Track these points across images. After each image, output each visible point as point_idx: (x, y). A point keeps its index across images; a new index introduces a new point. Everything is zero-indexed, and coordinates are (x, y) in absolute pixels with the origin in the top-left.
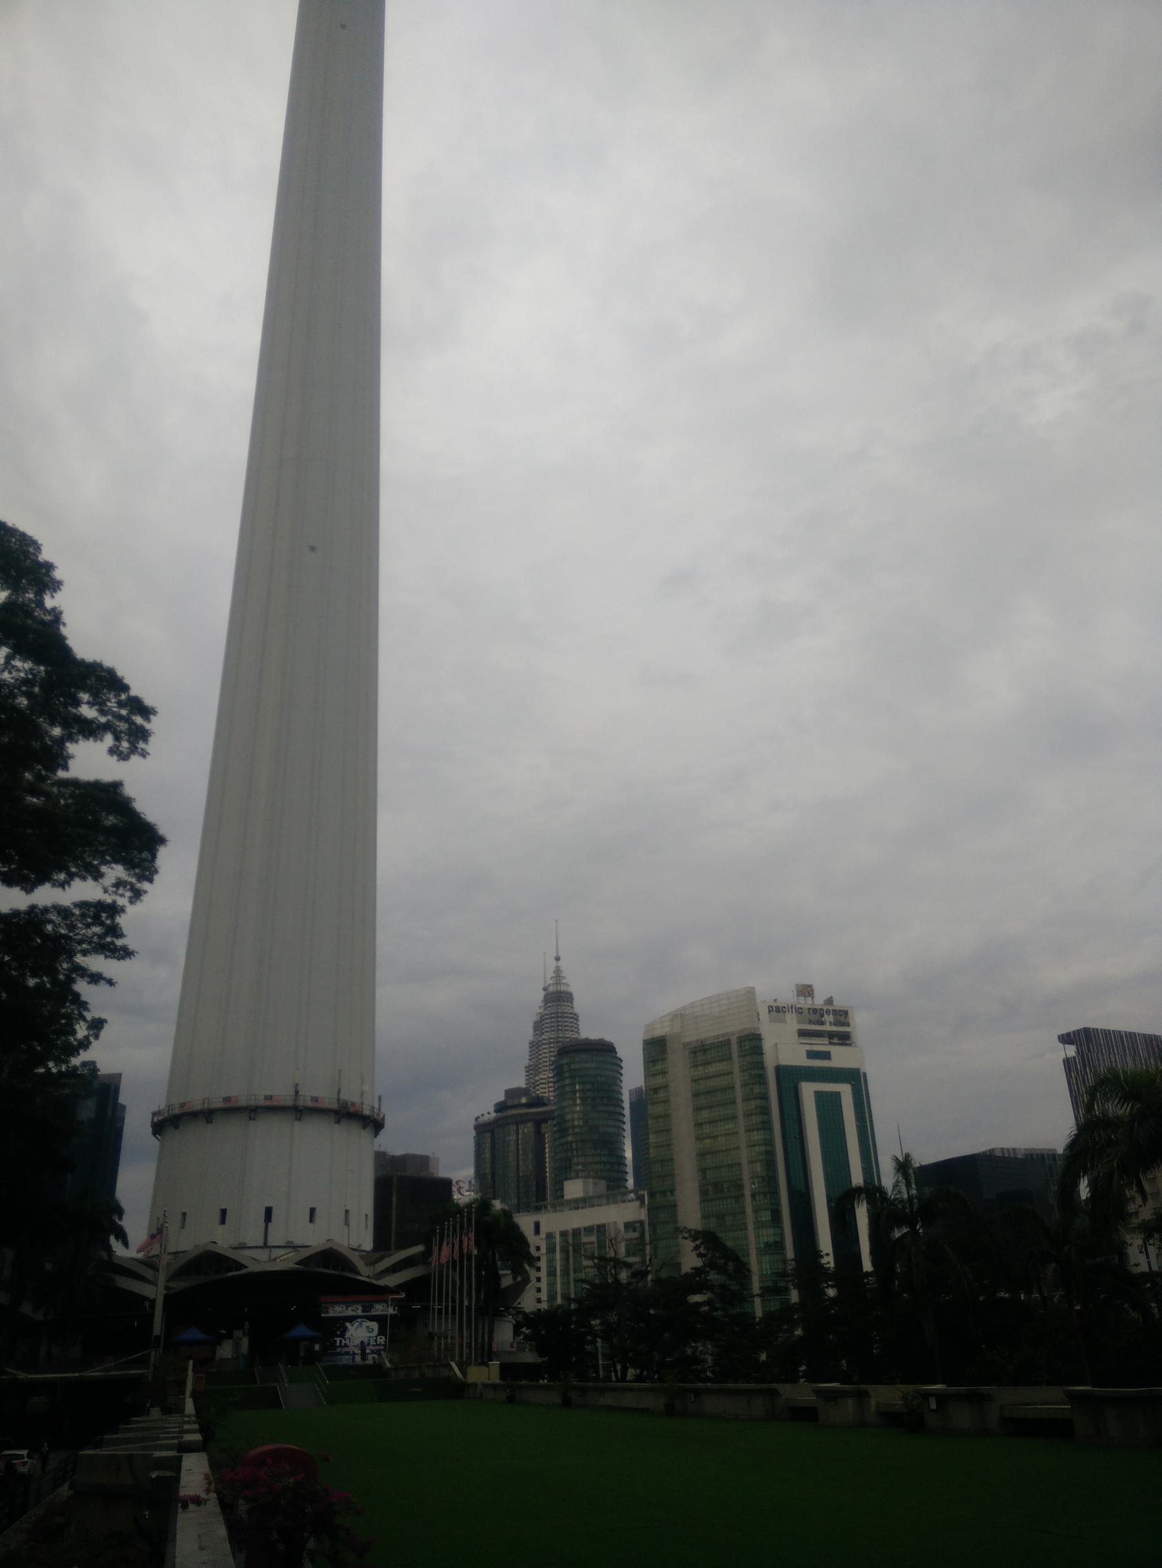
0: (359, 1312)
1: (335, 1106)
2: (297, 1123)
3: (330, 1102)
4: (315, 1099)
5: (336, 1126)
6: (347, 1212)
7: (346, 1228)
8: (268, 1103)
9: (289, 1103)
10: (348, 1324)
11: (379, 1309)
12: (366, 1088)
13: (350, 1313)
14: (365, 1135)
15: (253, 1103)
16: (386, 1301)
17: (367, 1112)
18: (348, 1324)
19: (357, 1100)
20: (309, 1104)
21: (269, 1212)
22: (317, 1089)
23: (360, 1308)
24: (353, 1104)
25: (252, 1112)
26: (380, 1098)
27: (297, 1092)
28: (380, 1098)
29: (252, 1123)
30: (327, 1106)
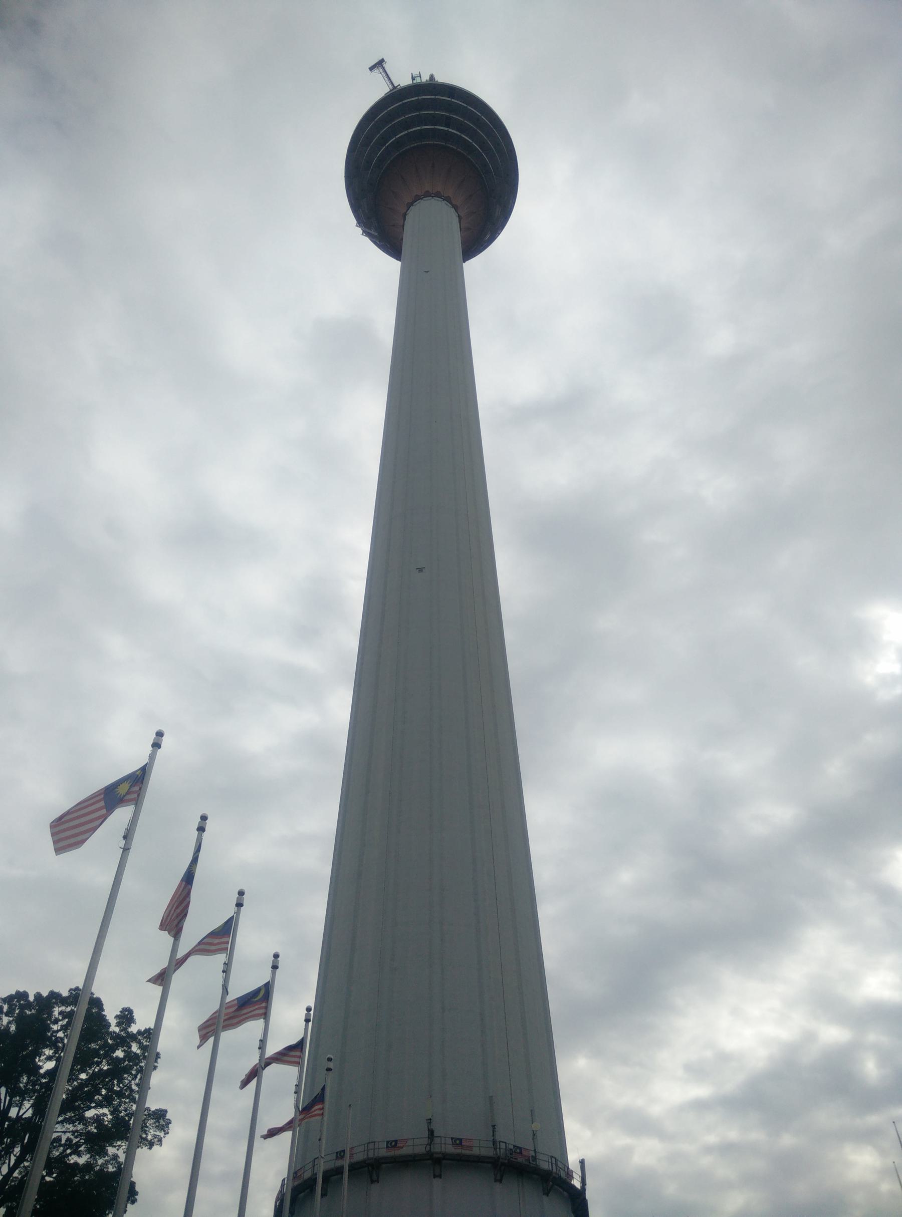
1: (490, 1153)
2: (437, 1182)
3: (482, 1149)
4: (458, 1142)
5: (498, 1186)
8: (392, 1153)
9: (420, 1150)
12: (536, 1126)
15: (371, 1155)
17: (545, 1166)
20: (451, 1149)
22: (461, 1124)
24: (519, 1150)
26: (582, 1162)
27: (431, 1132)
28: (582, 1162)
29: (375, 1187)
30: (476, 1151)
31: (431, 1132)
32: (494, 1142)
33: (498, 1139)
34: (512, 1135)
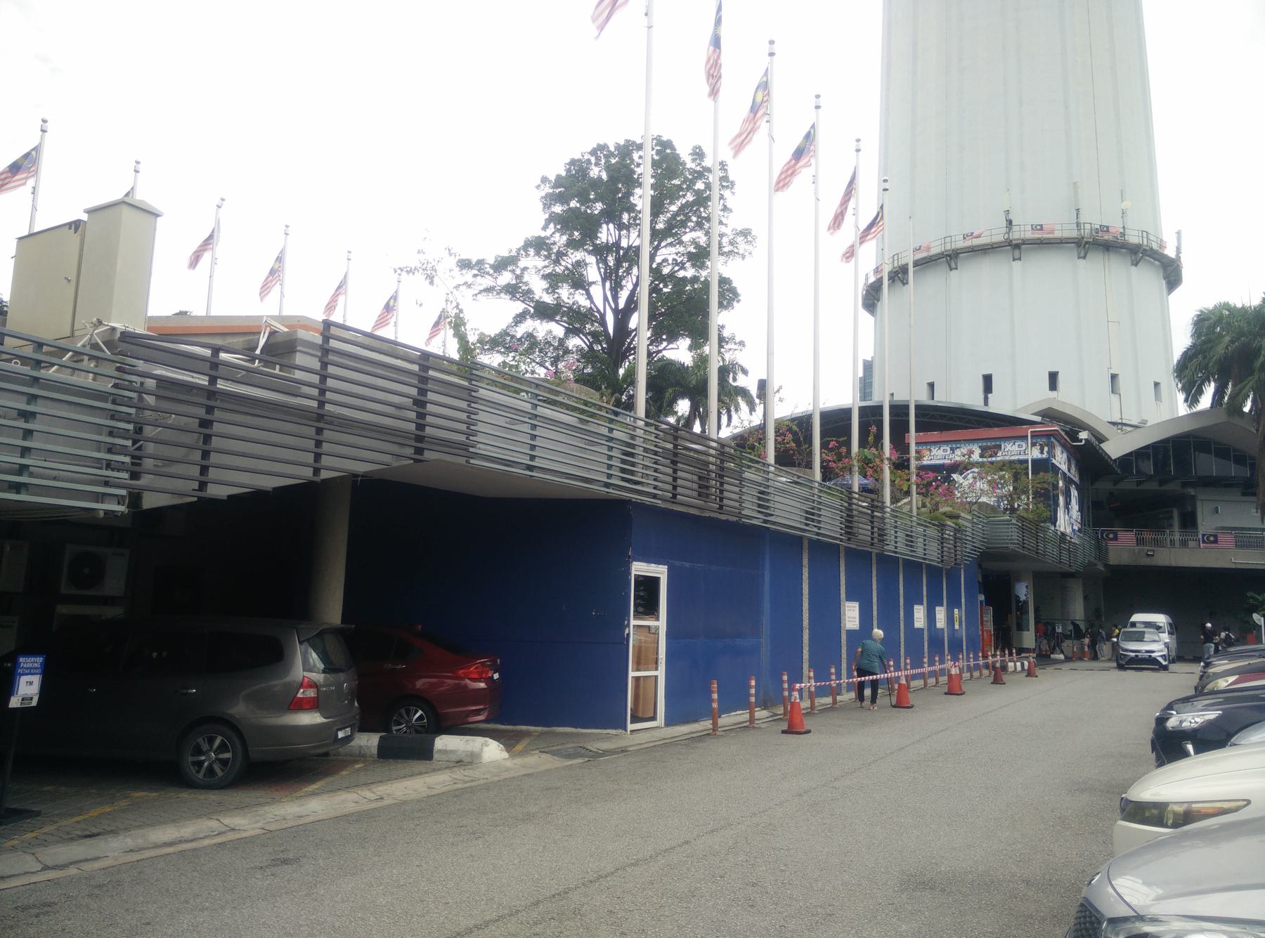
0: (976, 457)
6: (1114, 377)
7: (1115, 398)
9: (999, 238)
10: (955, 476)
11: (1011, 451)
12: (1126, 204)
13: (958, 456)
14: (1146, 279)
15: (948, 247)
16: (1024, 438)
17: (1133, 239)
18: (955, 476)
19: (1116, 225)
20: (1029, 235)
21: (988, 380)
23: (977, 452)
24: (1106, 229)
25: (951, 258)
26: (1179, 233)
27: (1010, 222)
30: (1058, 234)
31: (1010, 222)
32: (1078, 224)
33: (1082, 221)
34: (1100, 214)
